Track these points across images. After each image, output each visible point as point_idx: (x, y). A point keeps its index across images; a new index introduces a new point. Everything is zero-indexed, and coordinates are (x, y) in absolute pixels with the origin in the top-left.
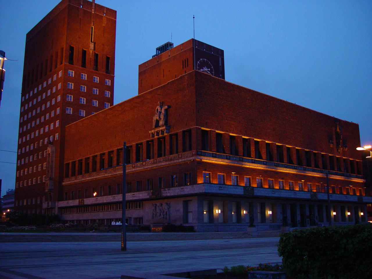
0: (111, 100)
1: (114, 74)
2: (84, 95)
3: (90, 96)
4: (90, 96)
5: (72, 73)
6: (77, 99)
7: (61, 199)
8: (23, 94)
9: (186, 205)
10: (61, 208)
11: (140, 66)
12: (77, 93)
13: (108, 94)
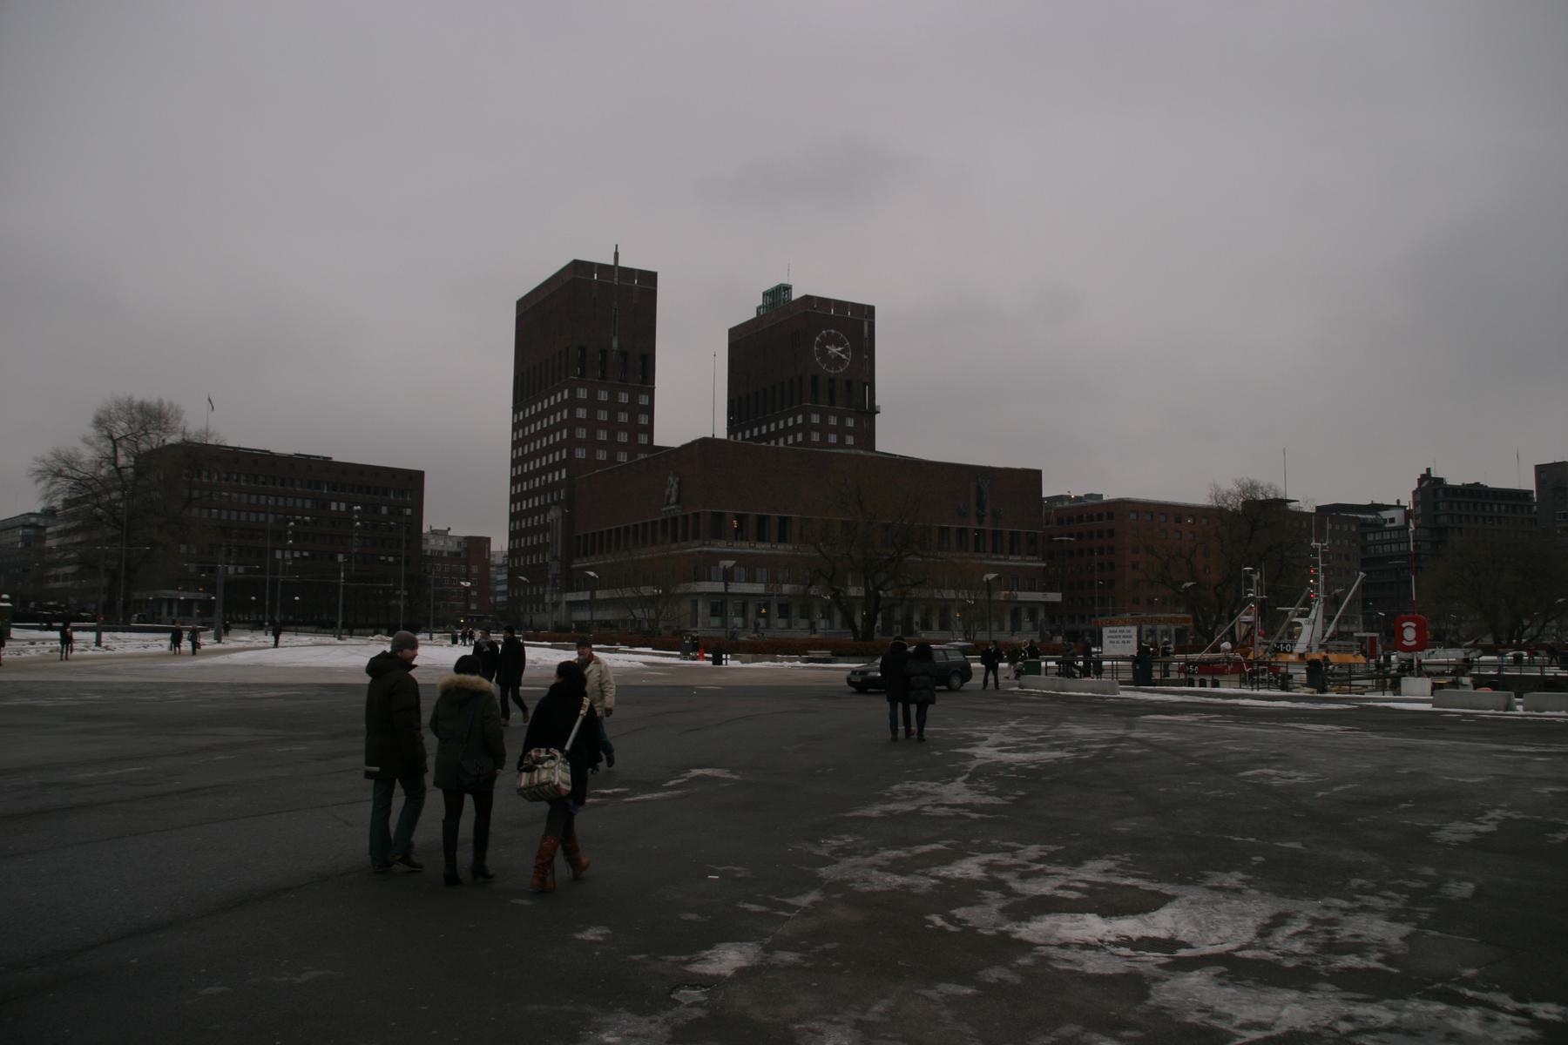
0: (649, 429)
1: (653, 383)
2: (603, 425)
3: (613, 427)
4: (613, 427)
5: (582, 394)
6: (592, 434)
7: (571, 590)
8: (516, 410)
9: (695, 604)
10: (570, 604)
11: (733, 332)
12: (592, 424)
13: (643, 420)
